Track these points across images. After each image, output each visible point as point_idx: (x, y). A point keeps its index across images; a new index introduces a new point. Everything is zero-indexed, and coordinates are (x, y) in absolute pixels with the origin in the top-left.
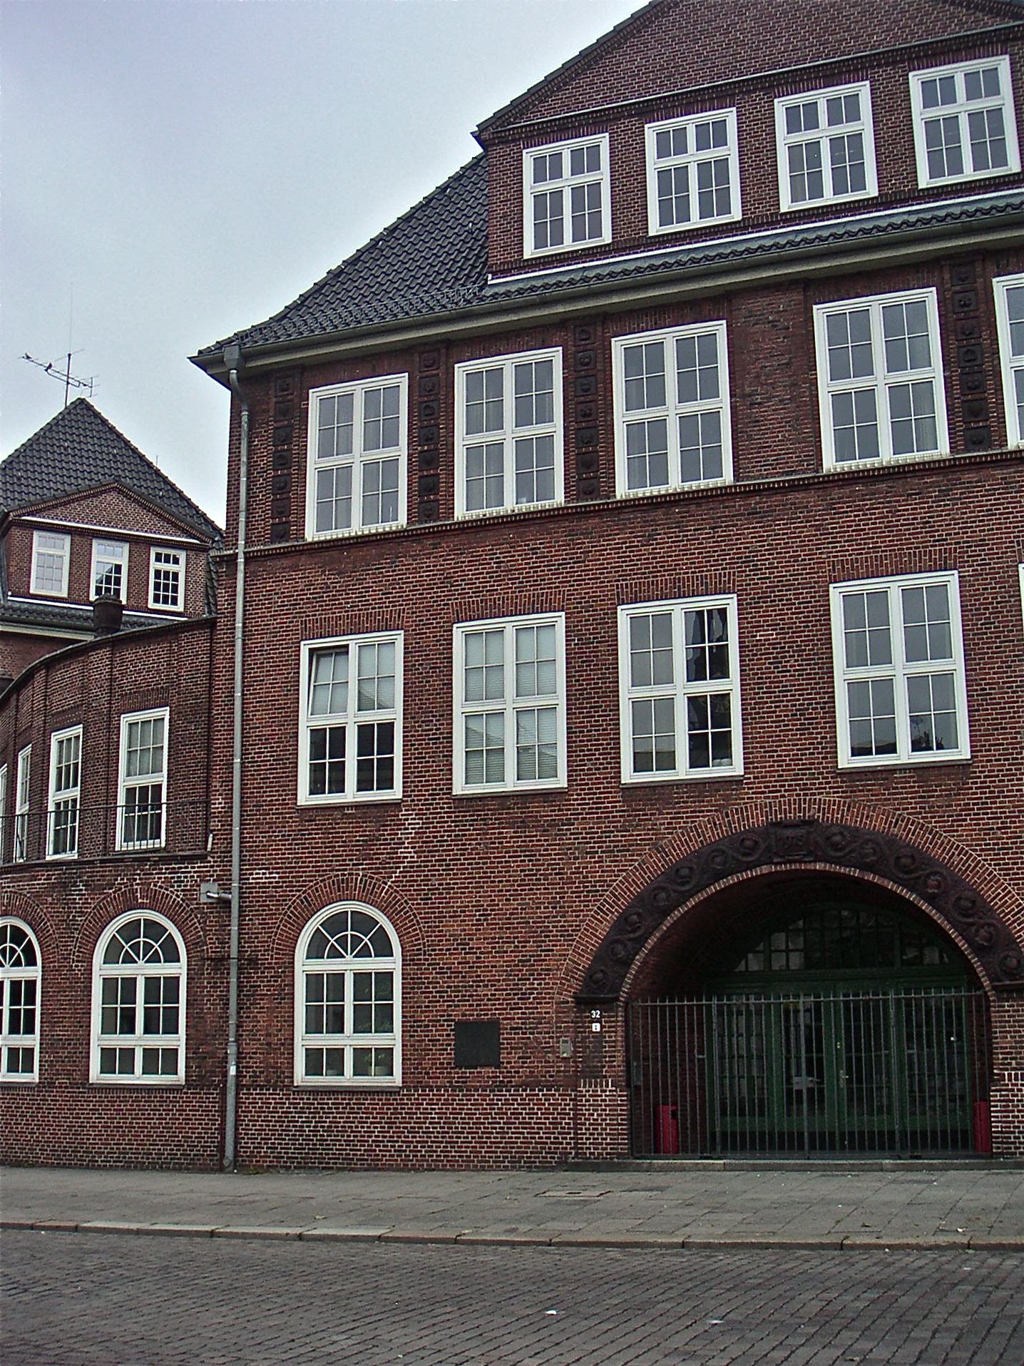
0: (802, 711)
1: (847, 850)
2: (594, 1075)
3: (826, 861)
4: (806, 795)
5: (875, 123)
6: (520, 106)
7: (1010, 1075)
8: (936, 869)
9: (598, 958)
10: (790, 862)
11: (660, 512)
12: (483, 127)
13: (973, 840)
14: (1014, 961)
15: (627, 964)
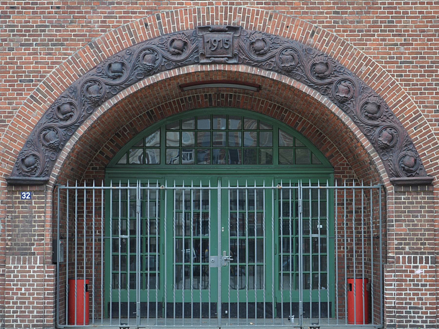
1: (269, 55)
2: (24, 252)
3: (248, 64)
7: (404, 258)
8: (346, 76)
9: (29, 143)
10: (214, 63)
13: (378, 53)
14: (412, 160)
15: (56, 149)
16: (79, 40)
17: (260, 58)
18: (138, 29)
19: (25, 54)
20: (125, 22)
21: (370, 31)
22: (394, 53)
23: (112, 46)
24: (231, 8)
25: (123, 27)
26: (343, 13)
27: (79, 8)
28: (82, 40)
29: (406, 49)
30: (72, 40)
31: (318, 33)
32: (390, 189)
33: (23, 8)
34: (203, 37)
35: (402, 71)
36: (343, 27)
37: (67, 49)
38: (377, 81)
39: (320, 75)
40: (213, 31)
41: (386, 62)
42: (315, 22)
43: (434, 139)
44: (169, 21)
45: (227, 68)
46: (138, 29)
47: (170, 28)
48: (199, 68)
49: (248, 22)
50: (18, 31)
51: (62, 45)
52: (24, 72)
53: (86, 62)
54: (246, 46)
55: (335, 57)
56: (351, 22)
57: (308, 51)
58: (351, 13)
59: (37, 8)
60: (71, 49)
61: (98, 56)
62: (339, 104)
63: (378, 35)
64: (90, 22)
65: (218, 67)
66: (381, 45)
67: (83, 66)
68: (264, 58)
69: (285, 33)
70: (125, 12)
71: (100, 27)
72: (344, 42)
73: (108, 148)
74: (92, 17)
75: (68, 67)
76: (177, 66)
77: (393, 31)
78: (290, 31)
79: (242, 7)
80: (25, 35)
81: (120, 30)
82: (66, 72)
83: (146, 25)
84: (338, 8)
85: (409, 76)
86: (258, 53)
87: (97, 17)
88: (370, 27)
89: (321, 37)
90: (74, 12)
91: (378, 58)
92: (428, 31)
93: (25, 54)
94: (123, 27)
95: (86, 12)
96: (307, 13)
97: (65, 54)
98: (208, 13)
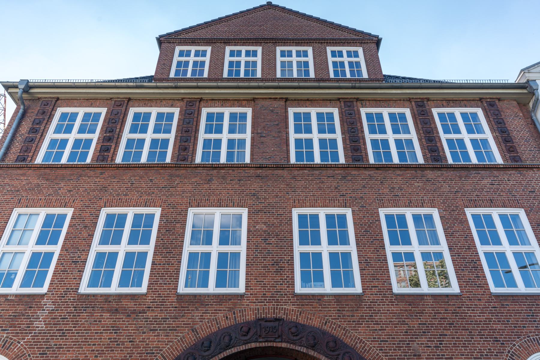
0: (277, 263)
3: (288, 342)
4: (278, 305)
5: (314, 58)
6: (177, 33)
11: (215, 171)
12: (161, 36)
13: (366, 335)
16: (186, 327)
17: (295, 338)
18: (222, 320)
19: (152, 336)
20: (214, 316)
21: (359, 321)
22: (376, 335)
23: (206, 331)
24: (277, 308)
25: (213, 319)
26: (343, 311)
27: (188, 307)
28: (188, 327)
29: (382, 333)
30: (182, 327)
31: (329, 323)
33: (155, 308)
34: (260, 324)
35: (382, 347)
36: (343, 319)
37: (178, 333)
38: (367, 353)
40: (266, 321)
41: (372, 341)
42: (327, 316)
44: (240, 315)
45: (275, 345)
46: (222, 320)
47: (241, 320)
48: (258, 345)
49: (287, 316)
50: (150, 321)
51: (175, 330)
52: (150, 347)
53: (189, 341)
55: (340, 338)
56: (348, 316)
57: (324, 333)
58: (347, 311)
59: (164, 307)
60: (181, 333)
61: (196, 337)
63: (365, 324)
64: (194, 316)
65: (270, 344)
66: (367, 330)
67: (187, 343)
68: (298, 337)
69: (309, 323)
70: (215, 310)
71: (199, 319)
72: (345, 328)
74: (195, 313)
75: (177, 344)
77: (373, 321)
78: (312, 322)
79: (284, 307)
80: (154, 324)
81: (211, 321)
82: (176, 348)
83: (227, 318)
84: (340, 308)
85: (386, 350)
87: (198, 313)
88: (359, 319)
89: (331, 325)
90: (185, 310)
91: (366, 338)
92: (394, 321)
93: (152, 336)
94: (213, 319)
95: (192, 310)
96: (321, 311)
97: (177, 336)
98: (264, 311)
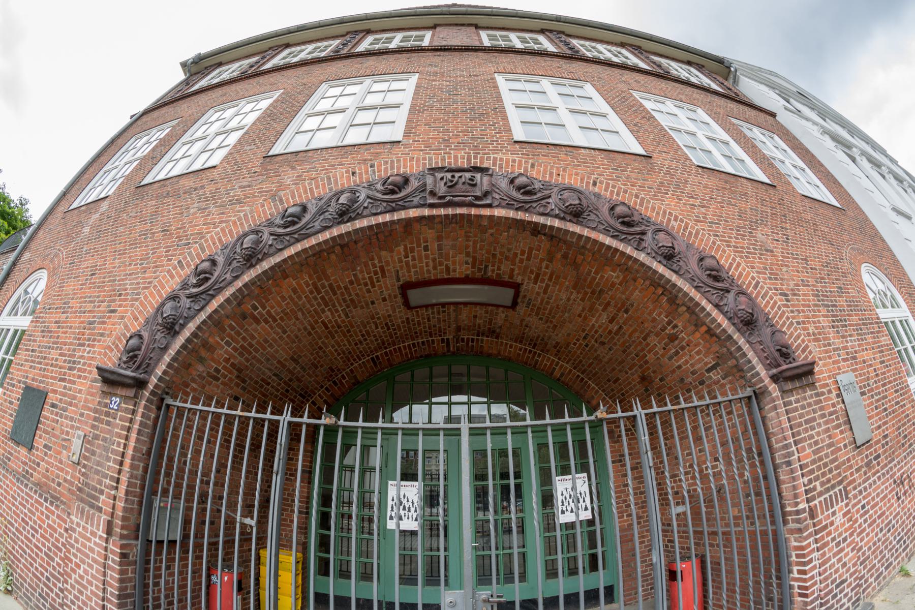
1: (539, 195)
3: (509, 206)
17: (527, 198)
32: (773, 387)
39: (626, 219)
43: (784, 312)
45: (473, 211)
54: (504, 184)
62: (665, 262)
73: (322, 398)
76: (389, 208)
86: (522, 191)
